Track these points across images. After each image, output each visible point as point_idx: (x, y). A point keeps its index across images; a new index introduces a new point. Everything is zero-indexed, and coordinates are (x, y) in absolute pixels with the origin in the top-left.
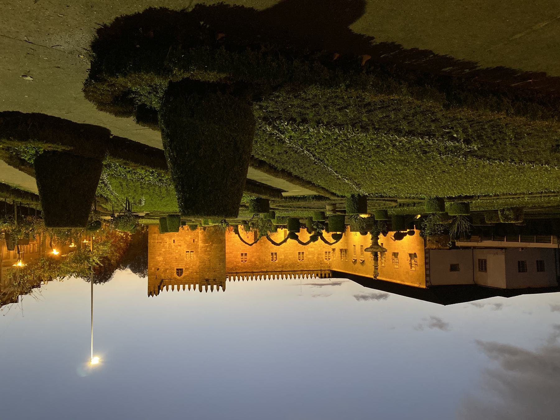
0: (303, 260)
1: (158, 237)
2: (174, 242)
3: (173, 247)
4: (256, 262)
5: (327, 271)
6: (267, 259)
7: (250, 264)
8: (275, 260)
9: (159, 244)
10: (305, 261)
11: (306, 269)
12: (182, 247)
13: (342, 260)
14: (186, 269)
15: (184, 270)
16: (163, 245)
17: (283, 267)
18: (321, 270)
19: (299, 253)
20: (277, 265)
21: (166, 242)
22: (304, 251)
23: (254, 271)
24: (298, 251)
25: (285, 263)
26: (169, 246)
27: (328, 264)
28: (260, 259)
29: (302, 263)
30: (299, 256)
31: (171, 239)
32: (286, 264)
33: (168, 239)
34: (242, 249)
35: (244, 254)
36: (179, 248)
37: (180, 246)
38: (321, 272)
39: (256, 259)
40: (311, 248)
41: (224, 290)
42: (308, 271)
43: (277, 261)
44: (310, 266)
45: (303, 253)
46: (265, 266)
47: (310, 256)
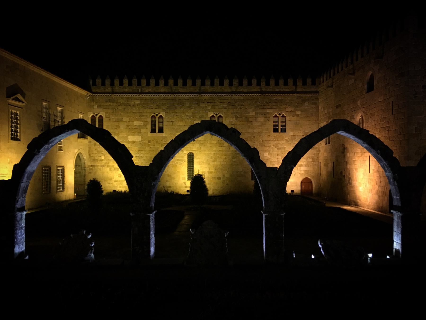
0: (153, 117)
4: (254, 114)
5: (98, 91)
6: (231, 119)
7: (268, 110)
8: (213, 116)
10: (149, 114)
11: (148, 96)
13: (59, 109)
17: (198, 102)
18: (113, 93)
19: (161, 130)
20: (209, 108)
22: (150, 134)
23: (258, 95)
24: (164, 134)
25: (192, 111)
27: (96, 107)
28: (247, 119)
29: (157, 110)
30: (161, 126)
32: (190, 107)
34: (285, 142)
35: (280, 130)
38: (113, 90)
39: (256, 120)
40: (134, 142)
42: (142, 93)
44: (138, 102)
45: (153, 131)
46: (236, 105)
47: (136, 123)
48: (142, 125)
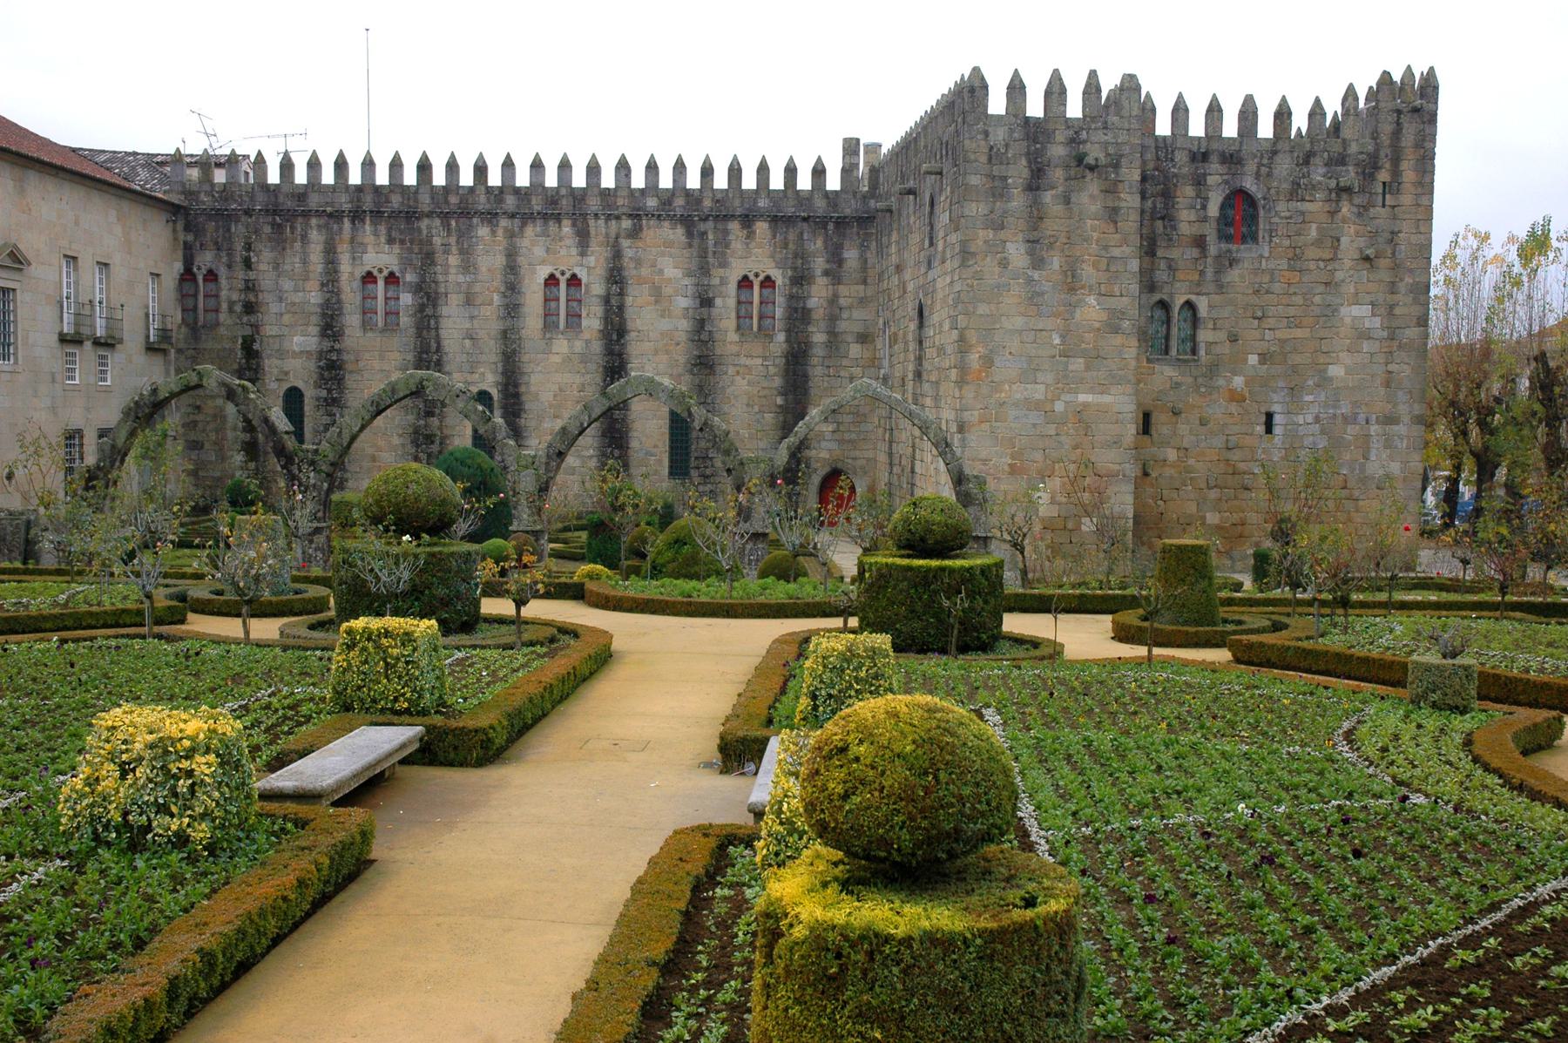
2: (1269, 417)
43: (543, 272)
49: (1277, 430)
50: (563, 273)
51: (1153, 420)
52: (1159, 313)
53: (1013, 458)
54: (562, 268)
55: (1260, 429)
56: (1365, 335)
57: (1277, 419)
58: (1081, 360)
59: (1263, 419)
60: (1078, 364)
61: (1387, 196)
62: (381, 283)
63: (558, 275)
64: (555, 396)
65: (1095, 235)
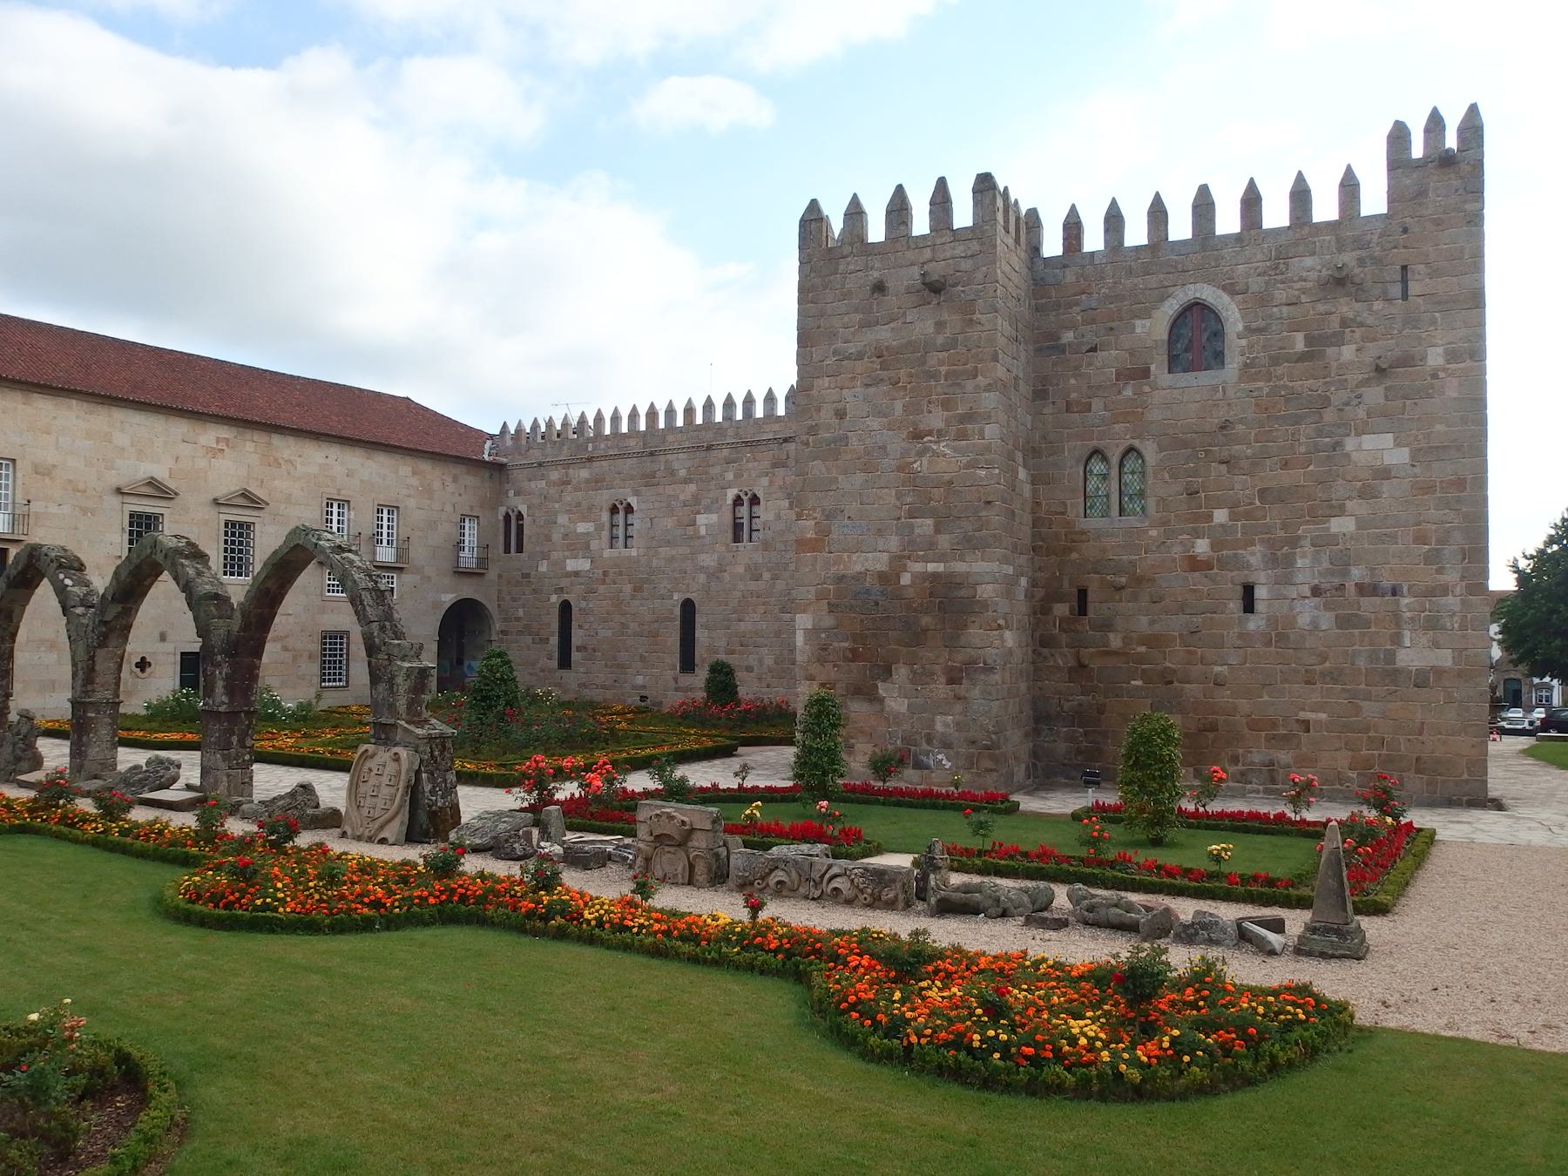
1: (1397, 640)
2: (1248, 591)
3: (1255, 555)
9: (1387, 583)
12: (1177, 551)
14: (1145, 373)
15: (1158, 368)
16: (1345, 573)
21: (1316, 591)
26: (1289, 561)
31: (1273, 621)
33: (1304, 620)
36: (1202, 547)
37: (1195, 564)
41: (812, 220)
43: (731, 494)
48: (592, 529)
49: (1260, 606)
50: (746, 495)
51: (1091, 596)
52: (1097, 467)
53: (854, 641)
54: (745, 489)
55: (1235, 605)
56: (1385, 473)
57: (1261, 593)
58: (930, 522)
59: (1240, 589)
60: (925, 526)
61: (1411, 284)
62: (622, 514)
63: (742, 495)
64: (739, 602)
65: (943, 369)
